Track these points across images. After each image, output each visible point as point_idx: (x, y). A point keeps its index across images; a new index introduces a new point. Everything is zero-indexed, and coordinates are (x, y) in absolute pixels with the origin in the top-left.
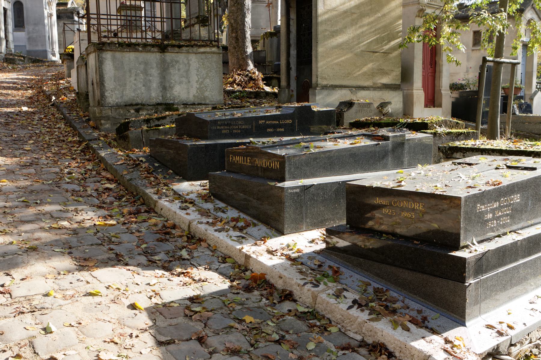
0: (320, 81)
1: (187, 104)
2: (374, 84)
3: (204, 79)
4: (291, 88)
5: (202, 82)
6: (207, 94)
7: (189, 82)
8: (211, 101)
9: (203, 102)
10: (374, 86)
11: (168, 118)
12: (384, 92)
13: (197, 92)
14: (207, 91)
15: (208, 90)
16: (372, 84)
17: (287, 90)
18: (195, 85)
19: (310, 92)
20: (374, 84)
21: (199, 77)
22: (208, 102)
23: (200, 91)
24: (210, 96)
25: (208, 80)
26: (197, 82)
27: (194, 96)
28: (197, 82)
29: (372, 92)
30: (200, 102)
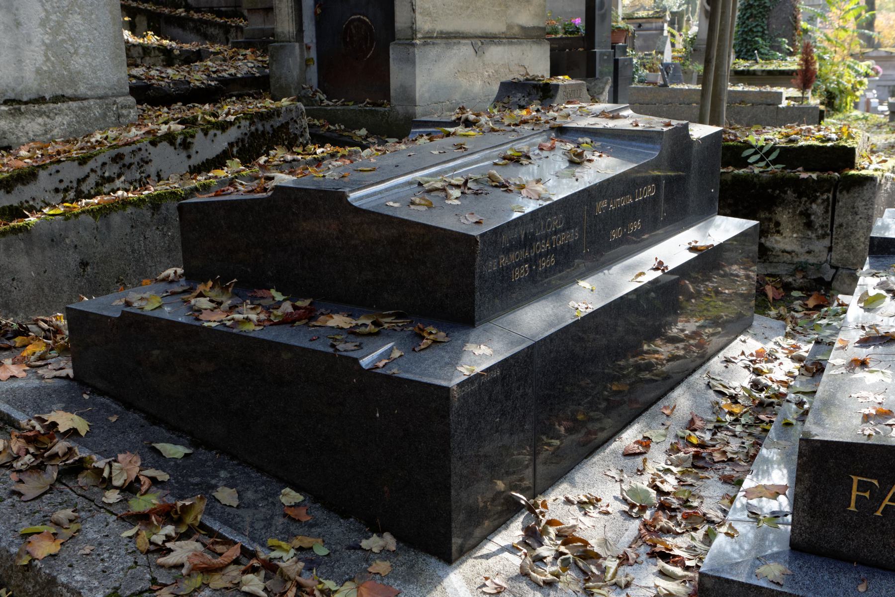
0: (424, 24)
1: (19, 102)
2: (510, 27)
3: (67, 13)
4: (307, 40)
5: (59, 25)
6: (78, 63)
7: (18, 24)
8: (93, 88)
9: (69, 92)
10: (508, 34)
11: (42, 174)
12: (524, 47)
13: (48, 59)
14: (76, 52)
15: (82, 51)
16: (504, 29)
17: (297, 45)
18: (39, 36)
19: (394, 52)
20: (510, 27)
21: (48, 6)
22: (82, 89)
23: (55, 55)
24: (87, 71)
25: (77, 18)
26: (43, 23)
27: (38, 71)
28: (43, 23)
29: (506, 48)
30: (60, 92)
